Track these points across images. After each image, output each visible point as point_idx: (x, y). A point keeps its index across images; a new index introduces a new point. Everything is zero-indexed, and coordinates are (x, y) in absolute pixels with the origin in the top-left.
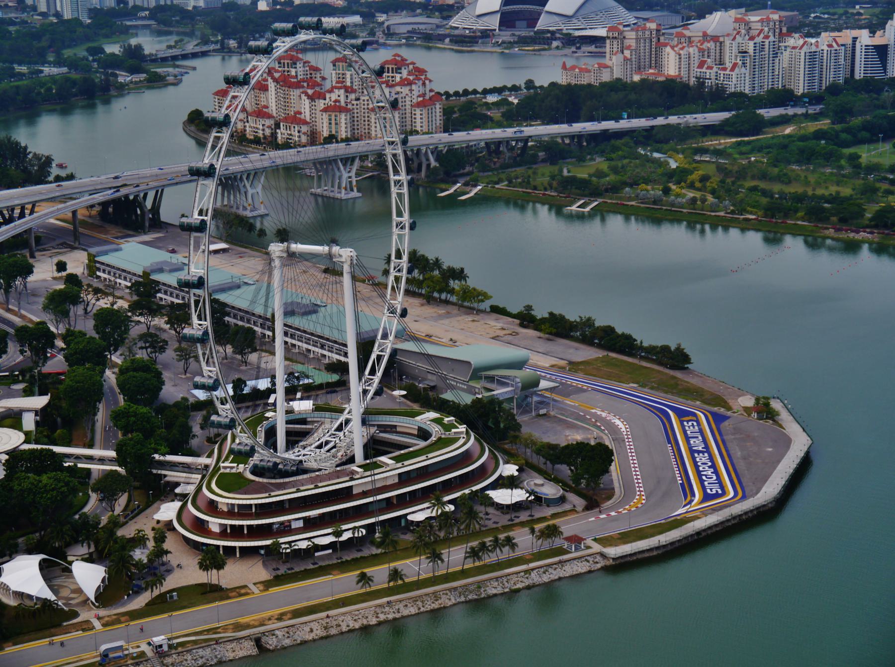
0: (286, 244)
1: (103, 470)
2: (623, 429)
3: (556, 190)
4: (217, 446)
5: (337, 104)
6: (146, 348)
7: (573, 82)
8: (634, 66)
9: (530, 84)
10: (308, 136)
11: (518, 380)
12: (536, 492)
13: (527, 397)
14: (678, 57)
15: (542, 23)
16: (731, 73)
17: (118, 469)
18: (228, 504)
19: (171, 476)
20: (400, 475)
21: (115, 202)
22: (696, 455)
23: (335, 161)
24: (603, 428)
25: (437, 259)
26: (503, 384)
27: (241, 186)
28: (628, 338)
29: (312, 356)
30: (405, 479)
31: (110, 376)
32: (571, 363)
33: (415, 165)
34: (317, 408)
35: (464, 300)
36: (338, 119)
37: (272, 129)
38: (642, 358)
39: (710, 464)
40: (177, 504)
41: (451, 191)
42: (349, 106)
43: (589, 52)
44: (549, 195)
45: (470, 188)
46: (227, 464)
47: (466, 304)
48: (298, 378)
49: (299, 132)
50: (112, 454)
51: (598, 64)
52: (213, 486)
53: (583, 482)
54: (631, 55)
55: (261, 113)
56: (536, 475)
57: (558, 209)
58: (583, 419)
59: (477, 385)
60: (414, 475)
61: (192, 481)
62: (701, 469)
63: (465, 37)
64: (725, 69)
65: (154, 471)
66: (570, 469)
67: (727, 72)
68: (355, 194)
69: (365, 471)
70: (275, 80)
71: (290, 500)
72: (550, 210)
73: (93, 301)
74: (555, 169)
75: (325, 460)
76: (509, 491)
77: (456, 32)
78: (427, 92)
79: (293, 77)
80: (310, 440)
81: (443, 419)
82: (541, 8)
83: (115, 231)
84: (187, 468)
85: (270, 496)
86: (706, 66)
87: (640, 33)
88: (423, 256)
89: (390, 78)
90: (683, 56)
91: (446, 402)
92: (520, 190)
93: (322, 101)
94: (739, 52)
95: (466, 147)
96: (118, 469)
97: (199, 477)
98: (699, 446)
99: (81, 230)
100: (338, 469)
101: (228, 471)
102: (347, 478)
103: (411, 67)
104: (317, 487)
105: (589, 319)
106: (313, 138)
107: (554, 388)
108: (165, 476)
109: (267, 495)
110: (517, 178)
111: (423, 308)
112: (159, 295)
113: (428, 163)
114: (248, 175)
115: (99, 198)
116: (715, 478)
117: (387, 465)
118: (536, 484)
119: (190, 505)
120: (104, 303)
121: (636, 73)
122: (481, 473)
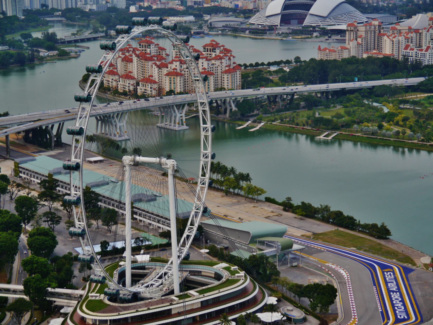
0: (133, 157)
1: (16, 298)
2: (346, 276)
3: (311, 126)
4: (88, 283)
5: (175, 71)
6: (48, 221)
7: (325, 58)
8: (364, 48)
9: (297, 59)
10: (156, 91)
11: (279, 244)
12: (288, 315)
13: (285, 254)
14: (391, 42)
15: (307, 22)
16: (425, 53)
17: (25, 297)
18: (92, 319)
19: (58, 302)
20: (202, 302)
21: (34, 130)
22: (392, 293)
23: (173, 106)
24: (332, 275)
25: (232, 168)
26: (271, 246)
27: (113, 121)
28: (351, 219)
29: (151, 227)
30: (205, 305)
31: (24, 238)
32: (314, 234)
33: (223, 110)
34: (152, 260)
35: (249, 194)
36: (175, 80)
37: (134, 86)
38: (359, 231)
39: (400, 299)
40: (61, 320)
41: (245, 126)
42: (183, 72)
43: (336, 40)
44: (306, 129)
45: (256, 124)
46: (93, 294)
47: (250, 196)
48: (142, 241)
49: (151, 88)
50: (21, 287)
51: (341, 47)
52: (84, 308)
53: (318, 309)
54: (362, 42)
55: (128, 76)
56: (288, 303)
57: (312, 138)
58: (320, 269)
59: (254, 247)
60: (210, 302)
61: (71, 305)
62: (394, 302)
63: (259, 30)
65: (48, 299)
66: (310, 301)
67: (423, 52)
68: (185, 127)
69: (180, 299)
70: (137, 56)
71: (132, 317)
72: (307, 138)
73: (16, 192)
74: (310, 113)
75: (156, 292)
76: (270, 313)
77: (253, 27)
78: (232, 64)
79: (148, 54)
80: (147, 280)
81: (230, 268)
82: (307, 12)
83: (33, 148)
84: (69, 297)
85: (119, 315)
86: (409, 48)
87: (368, 28)
88: (224, 166)
89: (209, 55)
90: (395, 42)
91: (234, 257)
92: (288, 125)
93: (166, 69)
95: (256, 99)
96: (25, 297)
97: (76, 302)
98: (393, 286)
99: (11, 147)
100: (163, 298)
101: (94, 298)
102: (168, 304)
103: (222, 48)
104: (149, 309)
105: (326, 207)
106: (160, 93)
107: (303, 249)
108: (55, 302)
109: (117, 314)
110: (286, 118)
111: (223, 198)
112: (58, 188)
113: (231, 108)
114: (118, 114)
115: (23, 127)
116: (403, 308)
117: (194, 296)
118: (288, 310)
119: (69, 321)
120: (23, 193)
121: (365, 53)
122: (254, 302)
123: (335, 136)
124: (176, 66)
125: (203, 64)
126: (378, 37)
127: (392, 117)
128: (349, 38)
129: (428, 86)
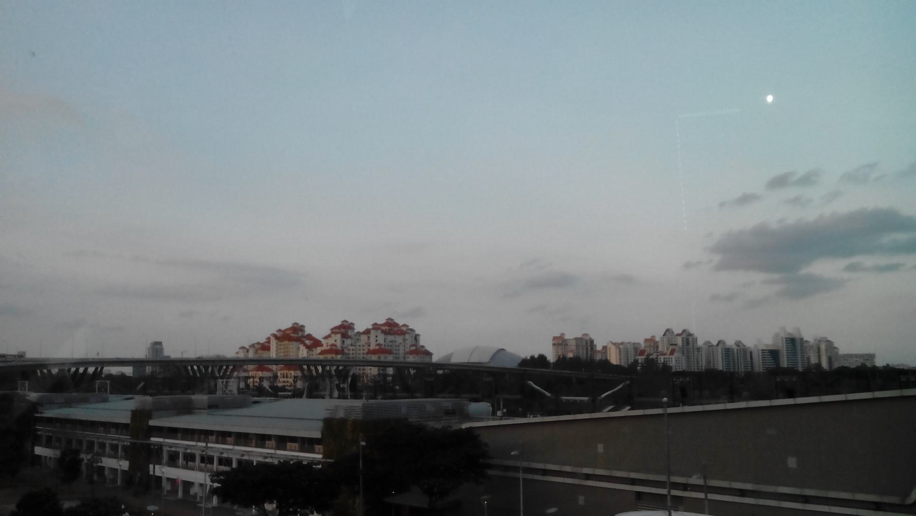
64: (665, 354)
94: (670, 345)
124: (336, 341)
125: (377, 338)
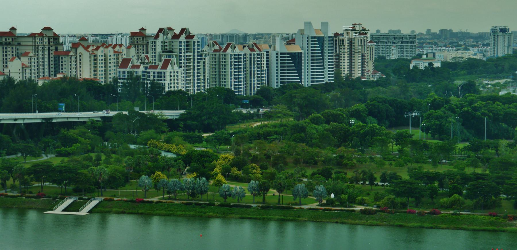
14: (93, 58)
16: (163, 71)
64: (156, 67)
67: (159, 70)
86: (130, 65)
94: (163, 52)
123: (96, 206)
126: (55, 58)
127: (206, 161)
128: (5, 57)
129: (203, 118)
